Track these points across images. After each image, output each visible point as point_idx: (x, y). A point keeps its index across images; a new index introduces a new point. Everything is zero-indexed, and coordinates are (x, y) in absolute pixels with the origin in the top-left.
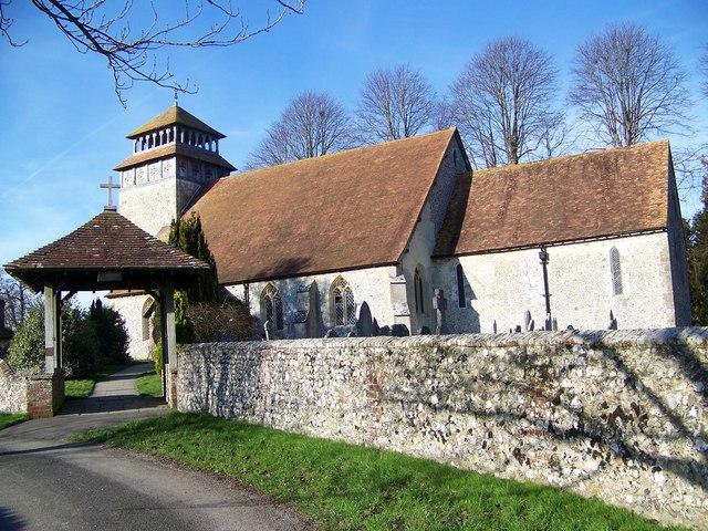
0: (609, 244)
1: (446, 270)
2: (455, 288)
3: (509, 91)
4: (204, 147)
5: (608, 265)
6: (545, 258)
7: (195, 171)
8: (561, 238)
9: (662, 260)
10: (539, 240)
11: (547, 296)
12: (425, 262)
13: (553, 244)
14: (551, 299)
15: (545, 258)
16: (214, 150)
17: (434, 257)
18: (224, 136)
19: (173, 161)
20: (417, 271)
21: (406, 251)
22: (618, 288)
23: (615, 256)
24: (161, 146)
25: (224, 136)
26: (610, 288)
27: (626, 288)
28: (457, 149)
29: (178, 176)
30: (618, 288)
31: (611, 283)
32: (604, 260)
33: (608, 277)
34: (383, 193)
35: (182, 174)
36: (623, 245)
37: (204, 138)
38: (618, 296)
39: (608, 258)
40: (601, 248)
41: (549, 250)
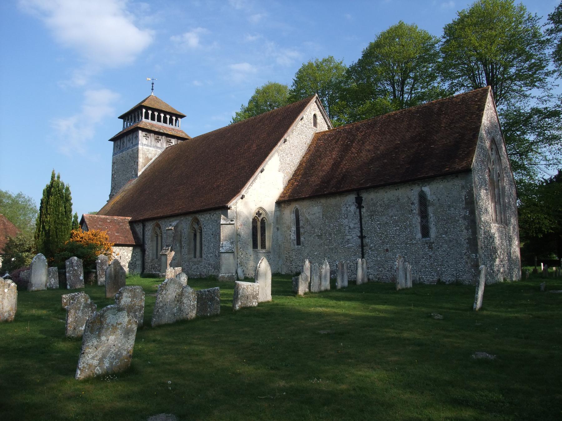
2: (294, 229)
5: (416, 208)
6: (359, 202)
11: (362, 237)
13: (367, 189)
14: (366, 241)
22: (425, 232)
23: (422, 198)
25: (182, 117)
26: (419, 235)
27: (433, 232)
30: (425, 232)
32: (413, 204)
33: (416, 220)
38: (424, 239)
41: (364, 196)
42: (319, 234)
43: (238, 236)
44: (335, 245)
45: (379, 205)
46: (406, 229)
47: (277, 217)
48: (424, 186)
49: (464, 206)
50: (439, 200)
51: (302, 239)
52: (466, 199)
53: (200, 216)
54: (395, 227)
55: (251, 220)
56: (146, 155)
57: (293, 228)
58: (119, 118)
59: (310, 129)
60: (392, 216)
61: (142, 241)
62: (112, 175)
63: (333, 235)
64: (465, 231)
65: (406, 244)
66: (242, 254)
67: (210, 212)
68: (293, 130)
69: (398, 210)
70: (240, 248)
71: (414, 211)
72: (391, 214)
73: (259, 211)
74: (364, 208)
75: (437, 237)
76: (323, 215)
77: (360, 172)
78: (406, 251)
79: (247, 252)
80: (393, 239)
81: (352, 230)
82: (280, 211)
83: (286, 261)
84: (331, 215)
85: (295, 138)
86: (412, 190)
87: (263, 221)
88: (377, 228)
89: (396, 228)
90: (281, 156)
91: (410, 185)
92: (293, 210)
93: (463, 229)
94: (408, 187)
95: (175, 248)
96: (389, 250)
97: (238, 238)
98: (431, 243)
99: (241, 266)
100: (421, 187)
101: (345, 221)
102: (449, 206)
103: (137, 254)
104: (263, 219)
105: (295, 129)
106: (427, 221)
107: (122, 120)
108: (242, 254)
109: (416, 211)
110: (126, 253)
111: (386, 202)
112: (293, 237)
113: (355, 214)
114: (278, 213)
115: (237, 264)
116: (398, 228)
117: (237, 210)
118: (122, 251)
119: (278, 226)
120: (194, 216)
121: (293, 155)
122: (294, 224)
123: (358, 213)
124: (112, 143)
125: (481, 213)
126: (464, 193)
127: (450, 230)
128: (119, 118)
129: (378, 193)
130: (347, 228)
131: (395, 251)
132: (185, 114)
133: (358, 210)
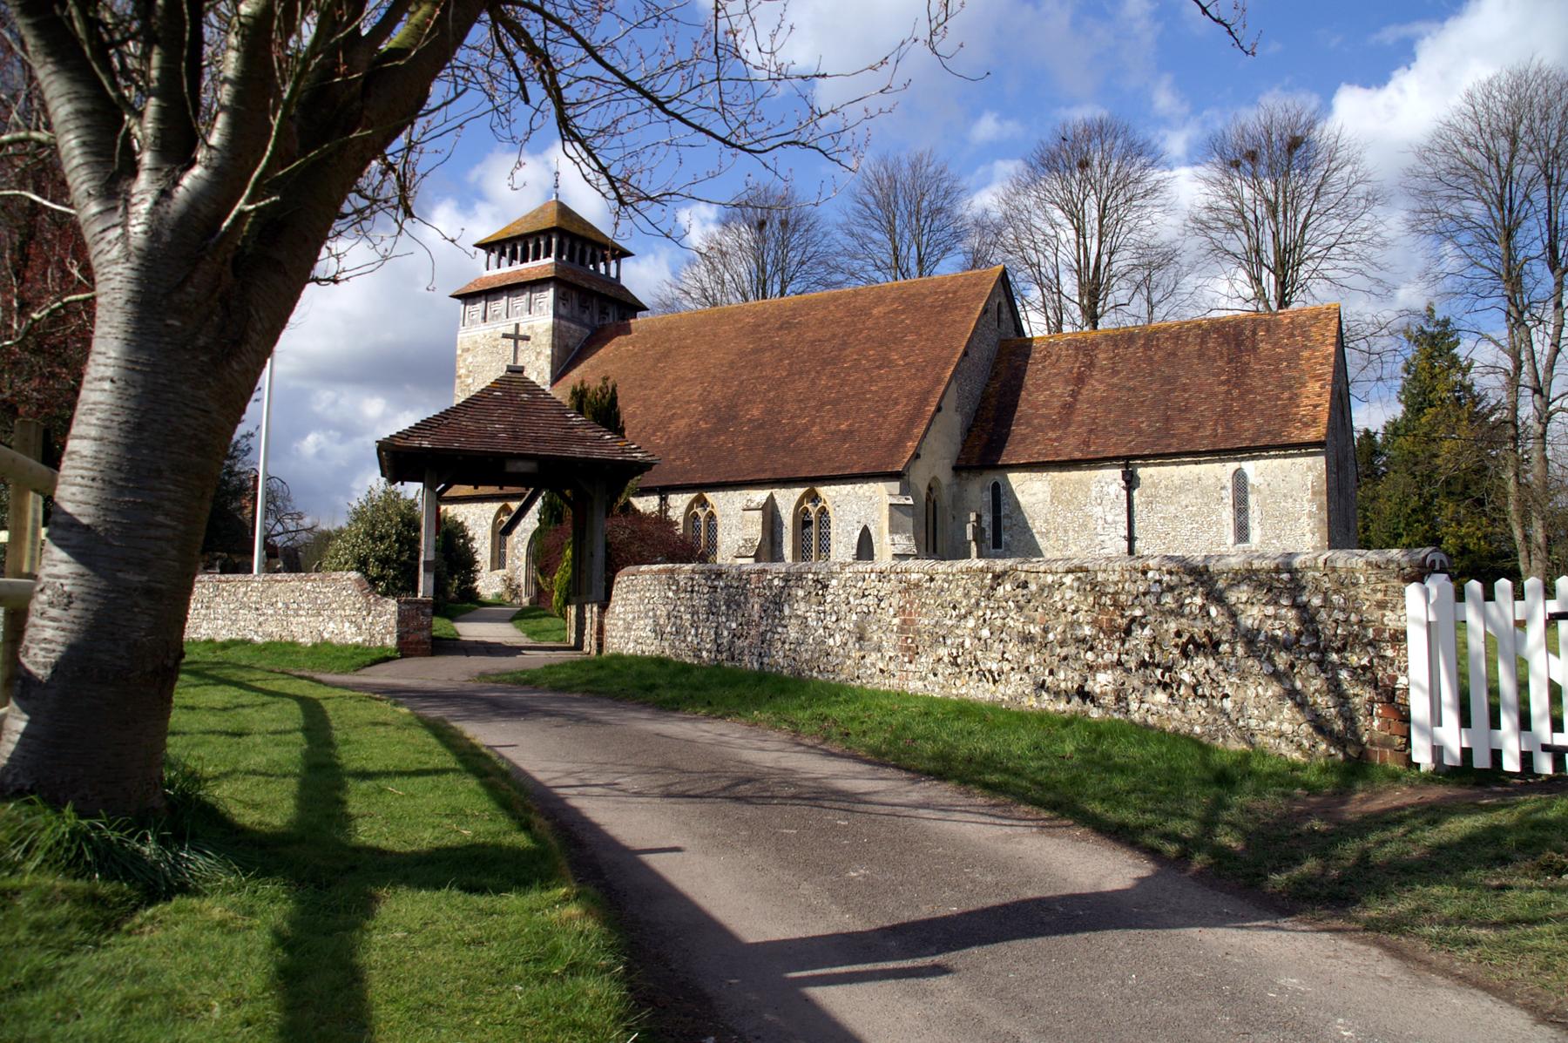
0: (1232, 466)
1: (977, 491)
3: (1092, 213)
4: (597, 269)
6: (1131, 482)
7: (583, 307)
8: (1158, 450)
9: (1314, 493)
10: (1123, 451)
12: (945, 476)
13: (1150, 458)
15: (1131, 482)
16: (613, 274)
17: (957, 469)
20: (930, 488)
21: (916, 456)
24: (531, 264)
26: (1231, 539)
28: (1004, 301)
29: (556, 315)
31: (1232, 526)
33: (1227, 514)
34: (886, 363)
35: (563, 311)
36: (1251, 468)
37: (599, 254)
38: (1241, 545)
39: (1229, 485)
40: (1223, 471)
41: (1143, 473)
46: (1210, 527)
51: (1005, 537)
52: (1313, 487)
63: (1071, 533)
64: (1309, 536)
71: (1226, 501)
72: (1184, 503)
75: (1263, 542)
76: (1053, 498)
82: (958, 484)
101: (1098, 511)
102: (1285, 496)
106: (1246, 518)
111: (1177, 482)
114: (955, 489)
126: (1310, 478)
132: (632, 251)
133: (1124, 493)
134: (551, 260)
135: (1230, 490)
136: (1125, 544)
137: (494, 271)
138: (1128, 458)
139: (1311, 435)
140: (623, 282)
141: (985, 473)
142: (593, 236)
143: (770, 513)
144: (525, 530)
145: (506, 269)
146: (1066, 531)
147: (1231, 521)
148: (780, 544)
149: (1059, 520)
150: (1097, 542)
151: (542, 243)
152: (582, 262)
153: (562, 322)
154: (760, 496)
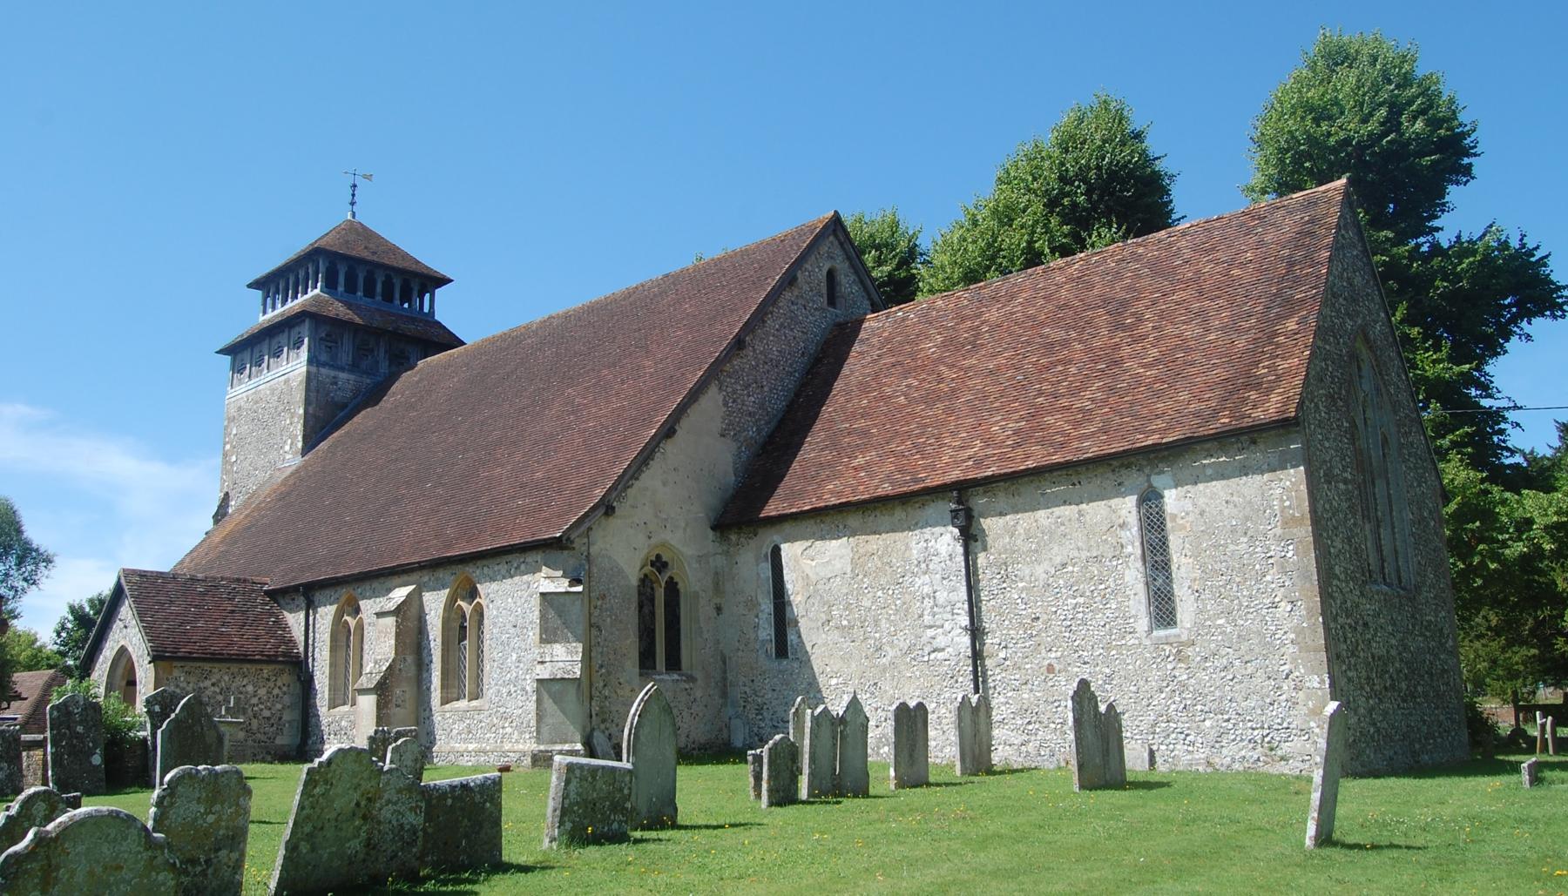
9: (1287, 523)
11: (976, 632)
16: (426, 309)
18: (443, 281)
19: (305, 328)
22: (1163, 610)
24: (301, 299)
25: (443, 281)
26: (1143, 623)
27: (1186, 609)
28: (842, 266)
30: (1163, 610)
31: (1142, 596)
33: (1133, 575)
38: (1162, 633)
42: (845, 623)
43: (594, 632)
44: (891, 653)
45: (1022, 531)
47: (717, 573)
48: (1159, 474)
49: (1278, 531)
50: (1202, 513)
52: (1283, 509)
53: (478, 572)
54: (1075, 597)
55: (634, 581)
56: (327, 395)
57: (763, 607)
58: (250, 286)
59: (817, 313)
60: (1064, 565)
61: (301, 649)
62: (225, 455)
63: (884, 624)
64: (1285, 607)
65: (1107, 648)
66: (605, 686)
67: (509, 557)
68: (766, 314)
69: (1080, 544)
70: (601, 666)
71: (1129, 549)
72: (1058, 560)
73: (658, 557)
74: (976, 541)
77: (965, 435)
78: (1107, 671)
79: (621, 680)
80: (1067, 634)
81: (941, 610)
83: (744, 707)
84: (879, 565)
85: (771, 338)
86: (1119, 484)
87: (672, 588)
88: (1019, 601)
89: (1074, 601)
90: (729, 390)
91: (1113, 471)
92: (764, 552)
93: (1277, 599)
94: (1110, 475)
95: (400, 670)
96: (1057, 667)
97: (593, 638)
98: (1182, 644)
99: (604, 721)
100: (1149, 476)
103: (285, 689)
104: (671, 578)
105: (771, 313)
106: (1169, 578)
107: (259, 293)
108: (605, 686)
109: (1134, 549)
110: (250, 688)
112: (767, 632)
113: (950, 560)
114: (720, 561)
115: (591, 717)
116: (1081, 600)
117: (591, 550)
118: (239, 681)
119: (718, 601)
120: (459, 569)
121: (766, 389)
122: (769, 592)
123: (960, 559)
124: (228, 358)
125: (1332, 550)
127: (1240, 604)
128: (250, 286)
129: (1019, 495)
130: (928, 603)
131: (1076, 669)
132: (449, 275)
133: (960, 550)
134: (317, 291)
135: (1135, 530)
136: (966, 640)
137: (270, 315)
138: (962, 489)
139: (1270, 407)
140: (437, 317)
141: (760, 531)
142: (401, 264)
143: (410, 622)
144: (104, 662)
145: (280, 310)
146: (877, 622)
147: (1140, 588)
148: (429, 670)
149: (866, 603)
150: (924, 639)
151: (310, 271)
152: (388, 297)
153: (324, 371)
154: (400, 594)
